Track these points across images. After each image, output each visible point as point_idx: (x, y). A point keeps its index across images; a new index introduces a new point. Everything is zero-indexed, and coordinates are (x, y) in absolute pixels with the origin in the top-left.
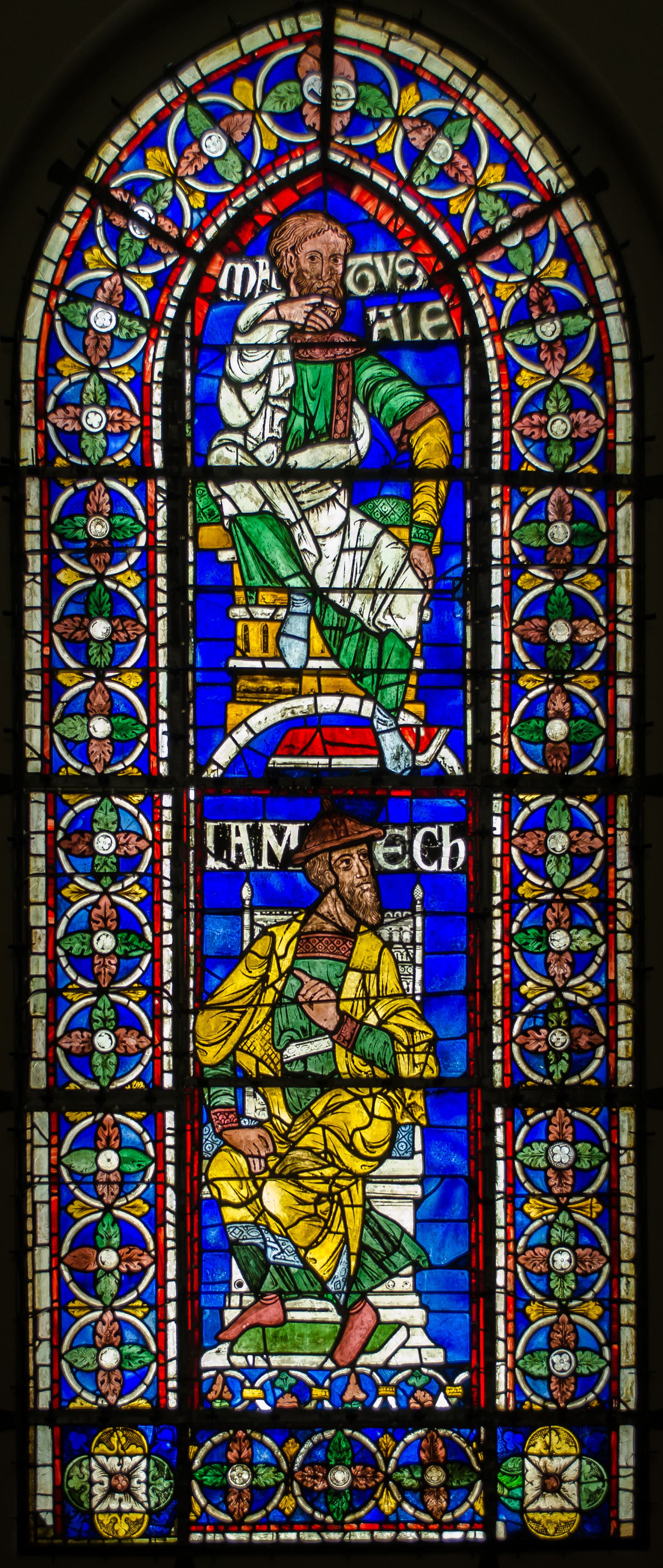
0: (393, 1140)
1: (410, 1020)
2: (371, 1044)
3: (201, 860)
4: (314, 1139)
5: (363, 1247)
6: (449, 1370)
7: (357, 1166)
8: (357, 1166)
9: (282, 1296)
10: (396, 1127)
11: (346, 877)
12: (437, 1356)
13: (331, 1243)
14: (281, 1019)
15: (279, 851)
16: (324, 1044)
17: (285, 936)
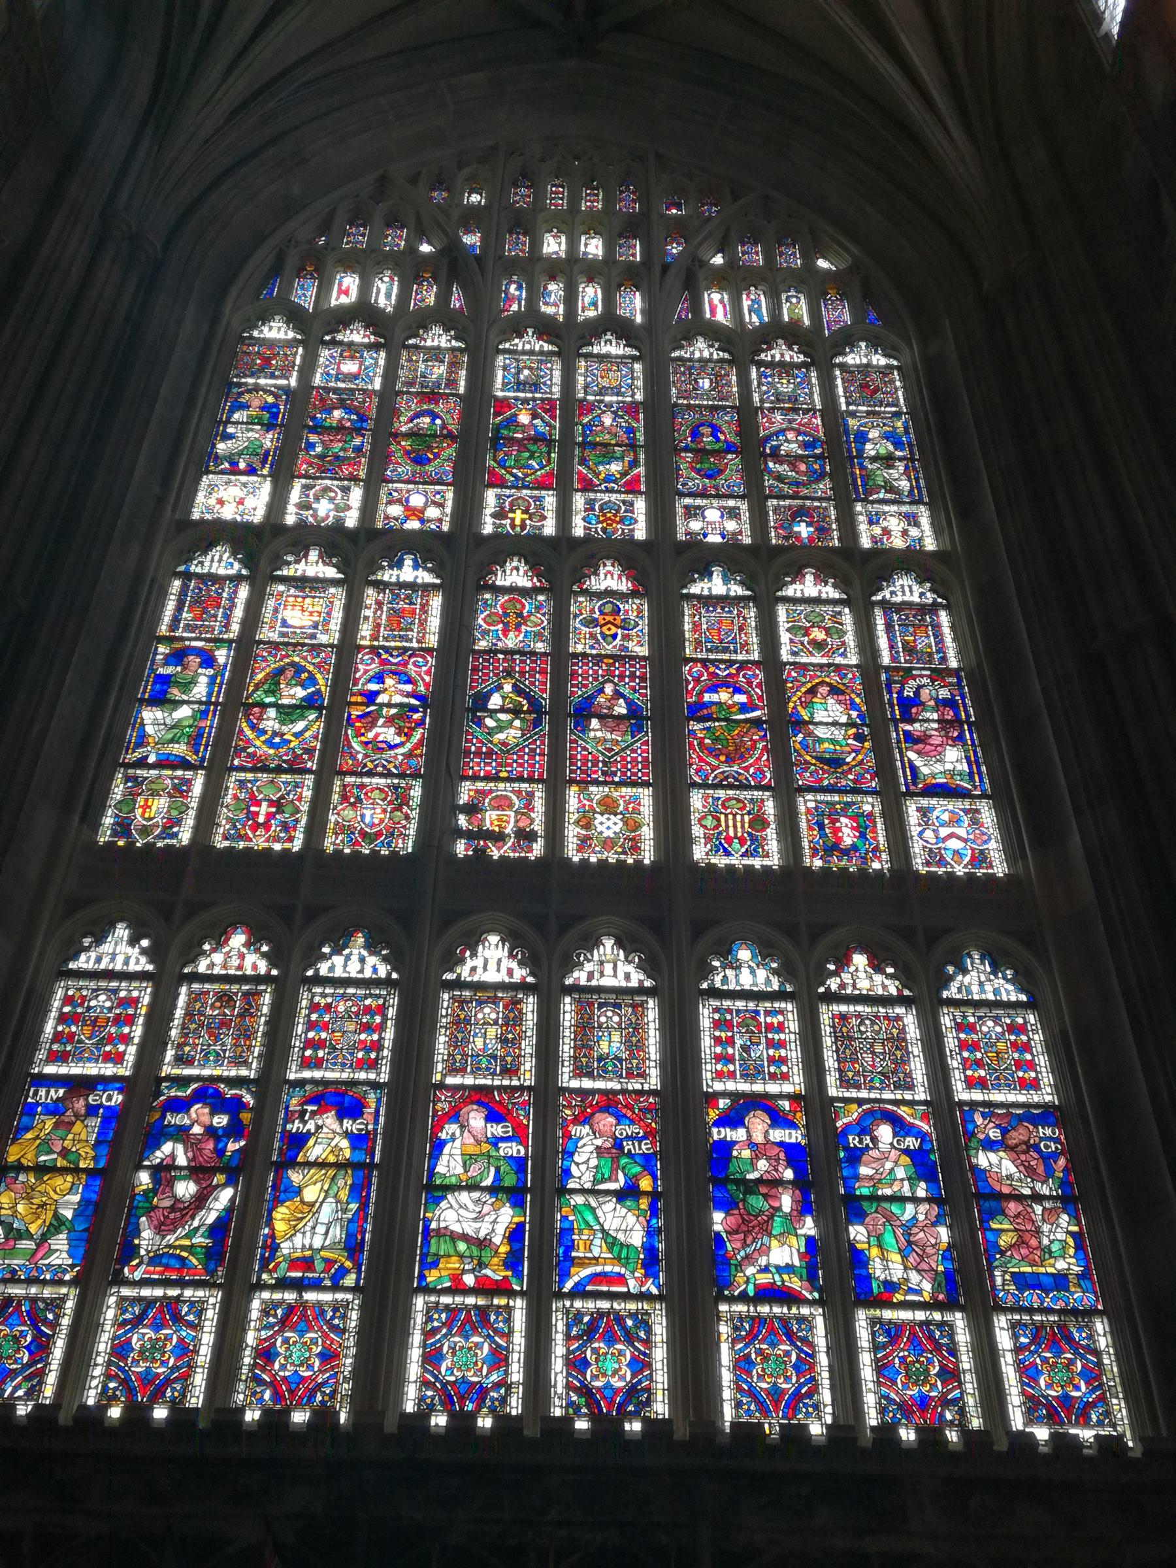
0: (71, 1189)
1: (88, 1150)
2: (72, 1157)
3: (26, 1099)
4: (41, 1188)
5: (51, 1224)
6: (72, 1266)
7: (56, 1197)
8: (56, 1197)
9: (15, 1239)
10: (73, 1184)
11: (76, 1105)
12: (70, 1262)
13: (40, 1222)
14: (41, 1148)
15: (55, 1097)
16: (55, 1156)
17: (49, 1124)
